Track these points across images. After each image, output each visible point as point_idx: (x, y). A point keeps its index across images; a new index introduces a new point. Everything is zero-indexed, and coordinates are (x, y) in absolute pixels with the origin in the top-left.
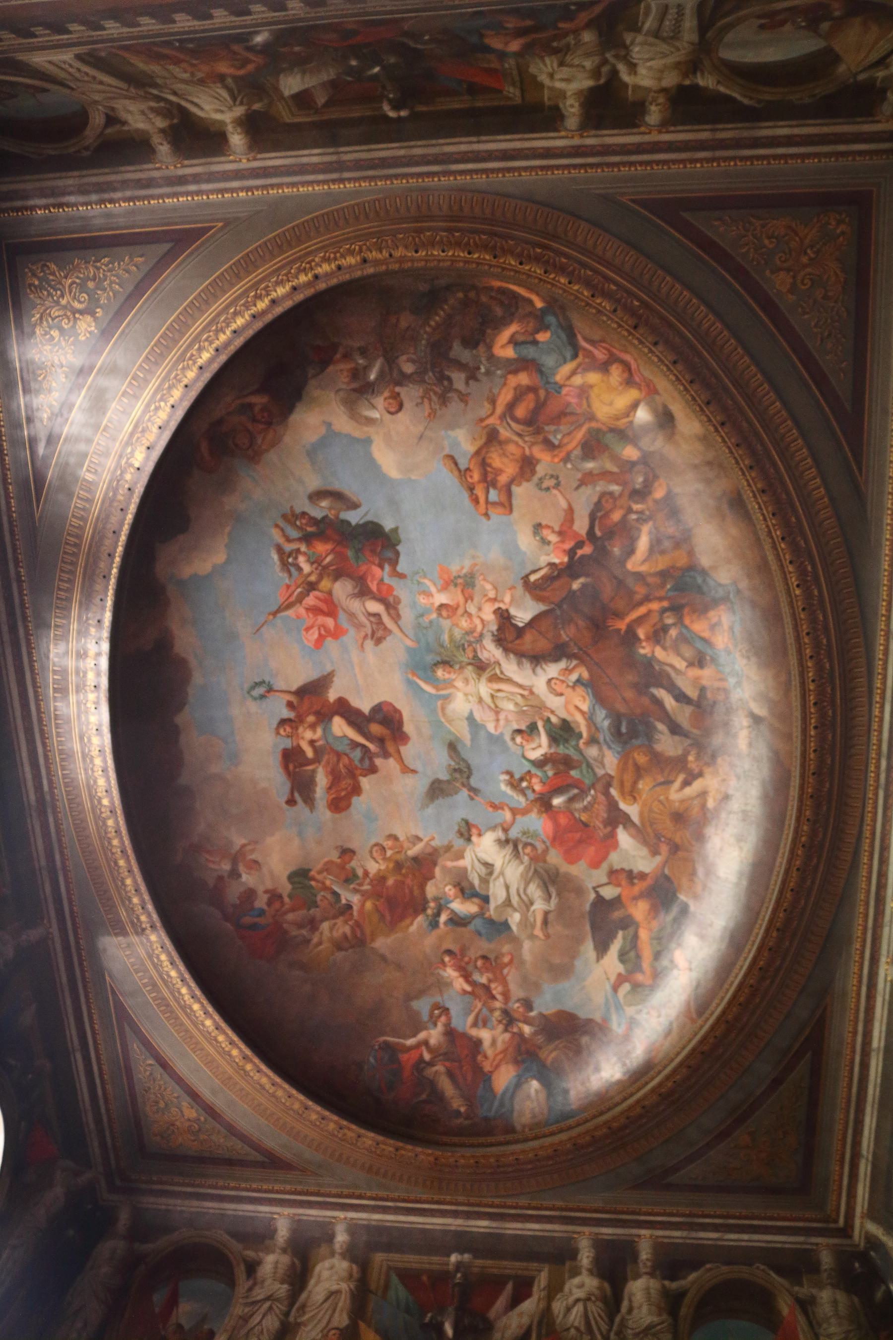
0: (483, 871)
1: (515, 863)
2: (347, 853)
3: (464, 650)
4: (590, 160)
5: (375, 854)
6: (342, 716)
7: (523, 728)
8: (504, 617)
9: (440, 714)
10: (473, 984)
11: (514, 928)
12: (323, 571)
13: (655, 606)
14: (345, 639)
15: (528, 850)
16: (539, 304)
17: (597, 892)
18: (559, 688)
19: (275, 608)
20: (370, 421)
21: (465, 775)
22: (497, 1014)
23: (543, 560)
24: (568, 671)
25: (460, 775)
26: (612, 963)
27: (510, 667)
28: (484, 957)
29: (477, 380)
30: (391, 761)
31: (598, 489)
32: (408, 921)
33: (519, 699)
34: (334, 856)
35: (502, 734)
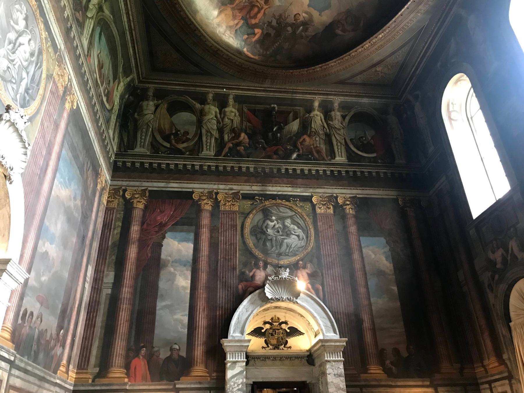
20: (306, 13)
29: (268, 22)
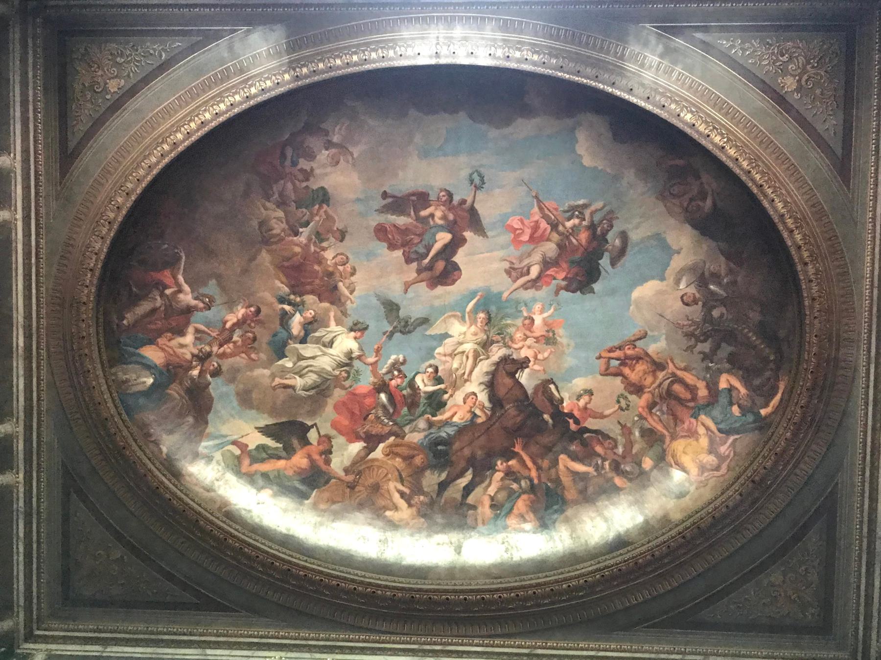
0: (327, 339)
1: (334, 364)
2: (342, 235)
3: (499, 334)
4: (868, 457)
5: (339, 257)
6: (452, 240)
7: (439, 374)
8: (523, 364)
9: (450, 314)
10: (232, 330)
11: (280, 362)
12: (565, 236)
13: (534, 474)
14: (512, 248)
15: (344, 374)
16: (763, 412)
17: (312, 426)
18: (470, 402)
19: (541, 198)
20: (678, 282)
21: (403, 329)
22: (208, 349)
23: (565, 395)
24: (483, 408)
25: (403, 326)
26: (256, 439)
27: (485, 366)
28: (255, 339)
29: (703, 360)
30: (414, 275)
31: (619, 438)
32: (284, 279)
33: (461, 372)
34: (339, 225)
35: (434, 358)
